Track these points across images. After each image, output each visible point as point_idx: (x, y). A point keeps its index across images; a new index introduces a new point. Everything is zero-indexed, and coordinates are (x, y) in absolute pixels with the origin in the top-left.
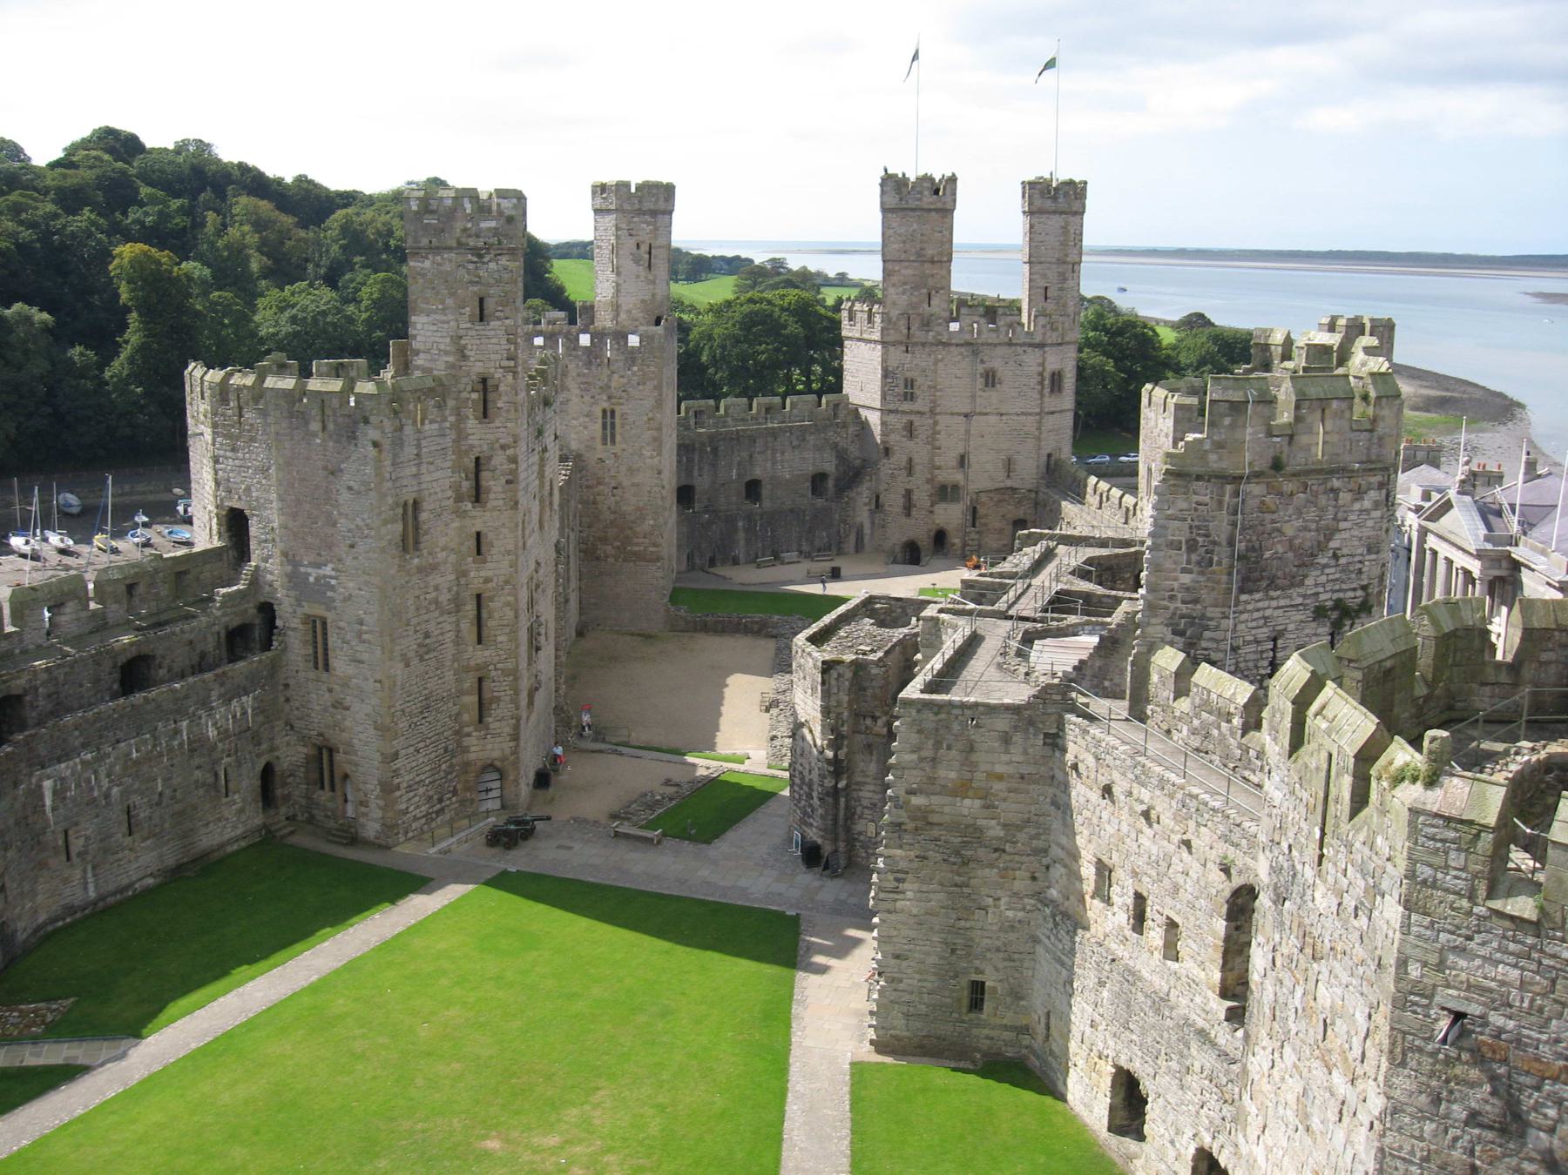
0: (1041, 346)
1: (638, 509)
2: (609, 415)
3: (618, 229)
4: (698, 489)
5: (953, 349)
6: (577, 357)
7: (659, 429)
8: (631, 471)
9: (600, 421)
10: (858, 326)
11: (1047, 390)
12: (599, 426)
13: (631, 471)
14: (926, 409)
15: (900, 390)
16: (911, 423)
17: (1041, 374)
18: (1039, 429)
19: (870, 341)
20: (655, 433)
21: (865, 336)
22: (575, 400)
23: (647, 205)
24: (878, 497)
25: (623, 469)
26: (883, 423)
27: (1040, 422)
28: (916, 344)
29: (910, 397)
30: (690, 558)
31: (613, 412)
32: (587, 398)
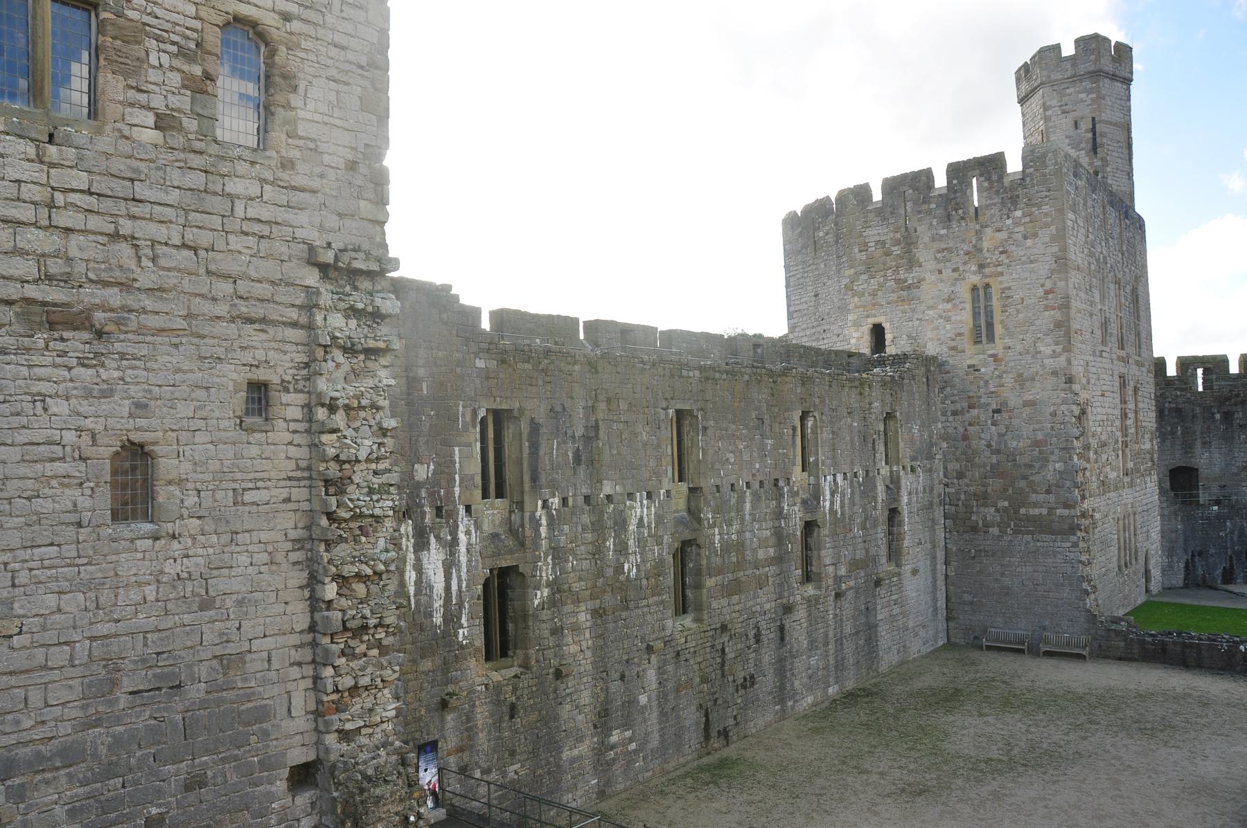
1: (1036, 443)
2: (980, 294)
3: (1045, 108)
4: (1203, 473)
6: (929, 212)
7: (1065, 306)
8: (1021, 380)
9: (969, 306)
12: (964, 317)
13: (1021, 380)
20: (1057, 315)
22: (931, 278)
23: (1082, 69)
25: (1008, 380)
30: (1189, 568)
32: (947, 273)
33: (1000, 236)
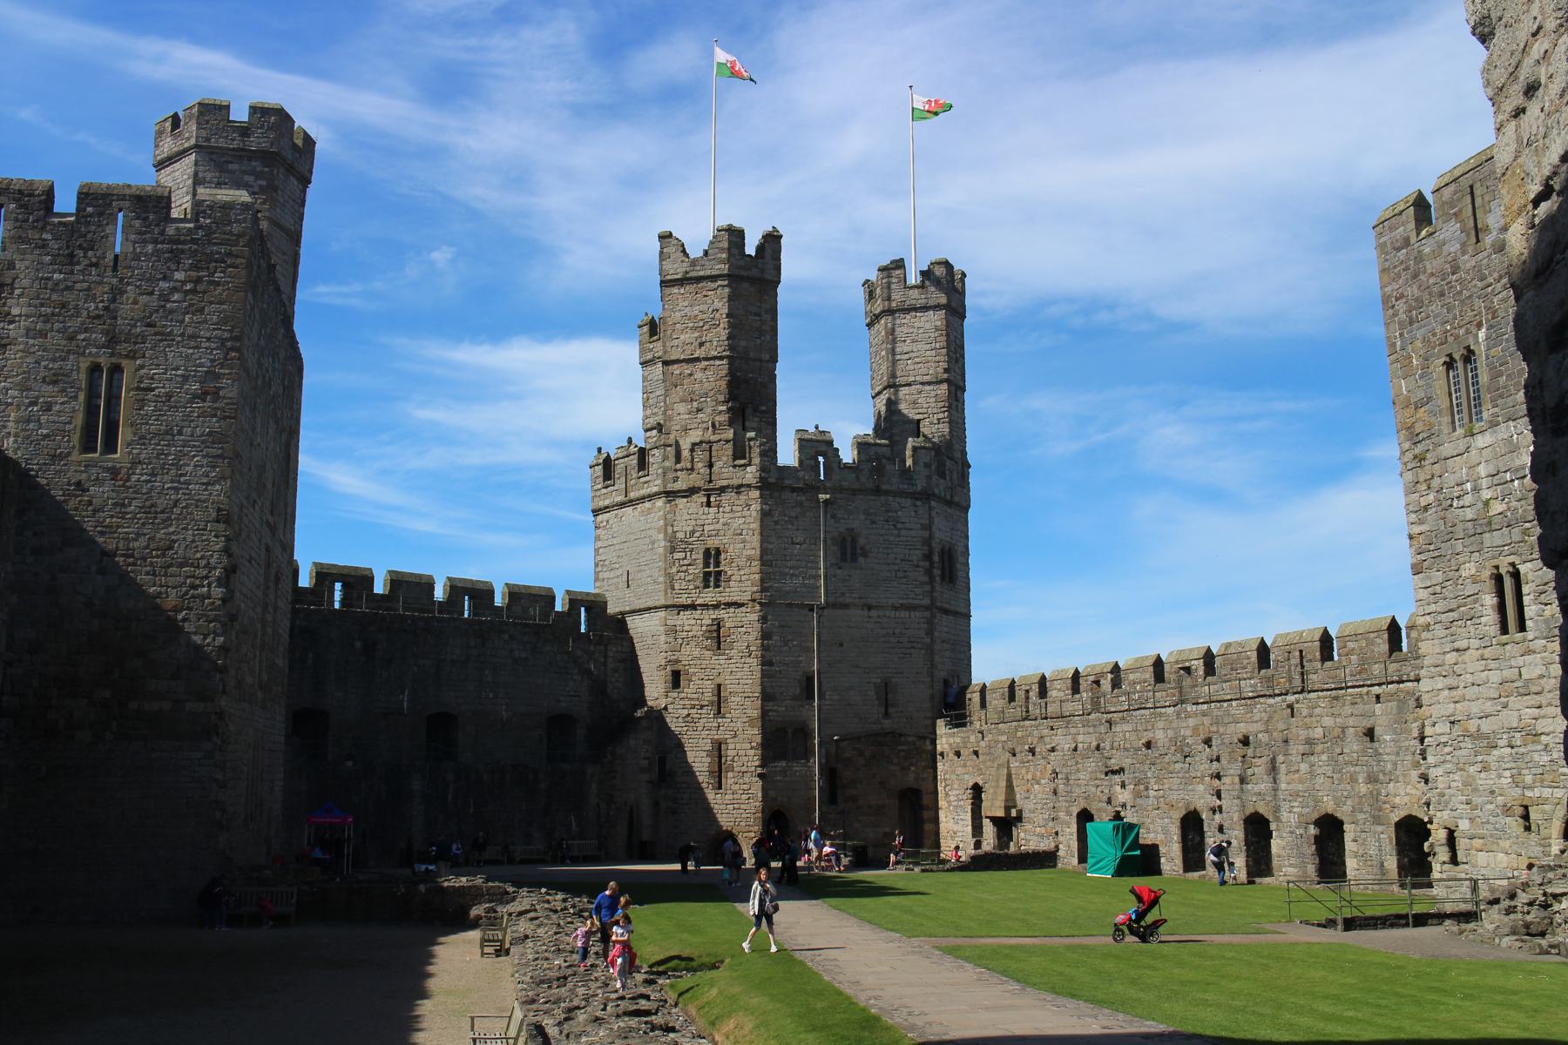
0: (926, 496)
5: (787, 495)
10: (620, 485)
11: (937, 572)
14: (746, 597)
15: (697, 570)
16: (718, 624)
17: (927, 542)
18: (930, 633)
19: (642, 499)
21: (632, 495)
24: (662, 762)
26: (672, 631)
27: (930, 622)
28: (723, 489)
29: (713, 578)
31: (116, 370)
32: (55, 339)
33: (144, 299)
